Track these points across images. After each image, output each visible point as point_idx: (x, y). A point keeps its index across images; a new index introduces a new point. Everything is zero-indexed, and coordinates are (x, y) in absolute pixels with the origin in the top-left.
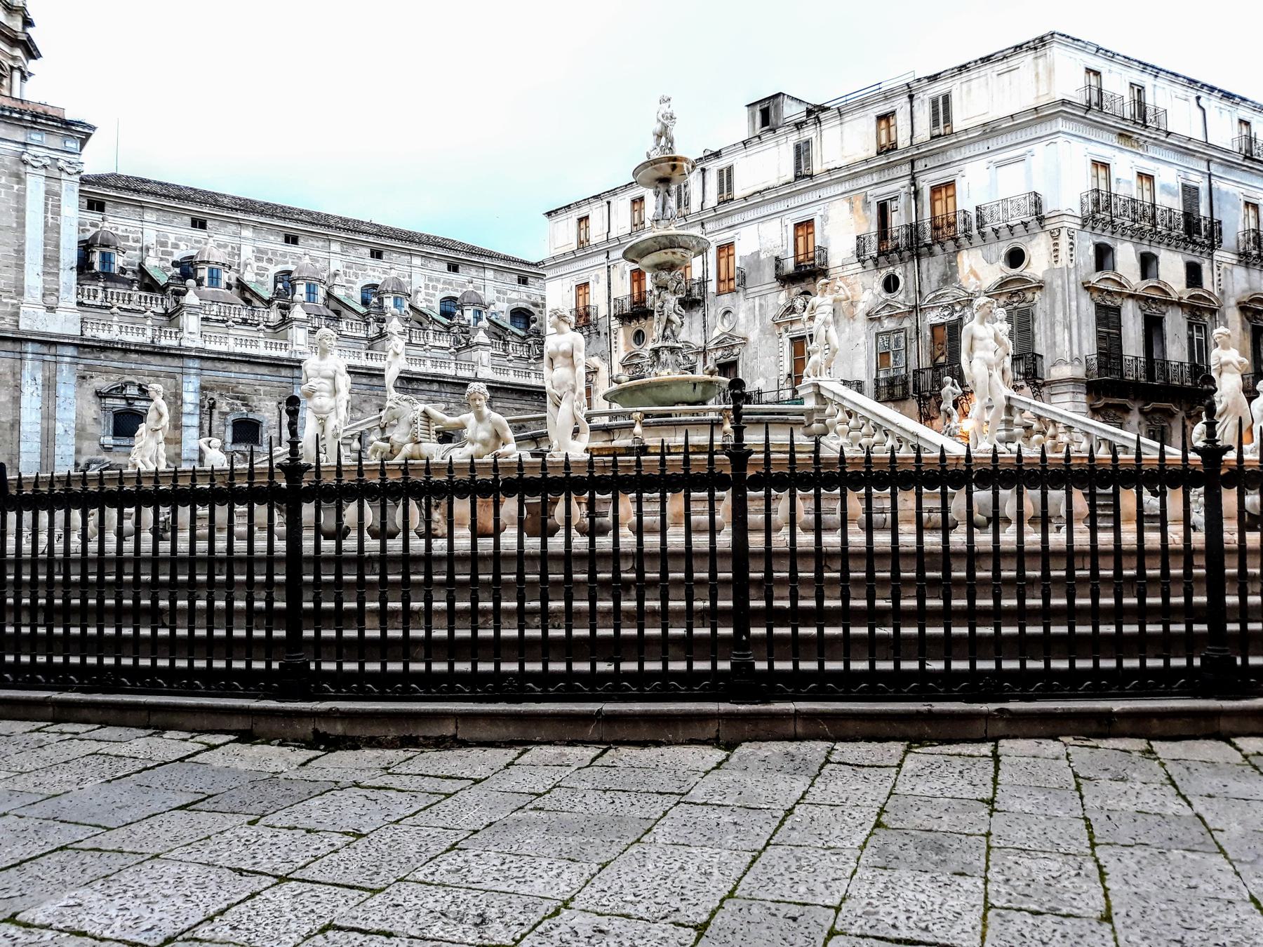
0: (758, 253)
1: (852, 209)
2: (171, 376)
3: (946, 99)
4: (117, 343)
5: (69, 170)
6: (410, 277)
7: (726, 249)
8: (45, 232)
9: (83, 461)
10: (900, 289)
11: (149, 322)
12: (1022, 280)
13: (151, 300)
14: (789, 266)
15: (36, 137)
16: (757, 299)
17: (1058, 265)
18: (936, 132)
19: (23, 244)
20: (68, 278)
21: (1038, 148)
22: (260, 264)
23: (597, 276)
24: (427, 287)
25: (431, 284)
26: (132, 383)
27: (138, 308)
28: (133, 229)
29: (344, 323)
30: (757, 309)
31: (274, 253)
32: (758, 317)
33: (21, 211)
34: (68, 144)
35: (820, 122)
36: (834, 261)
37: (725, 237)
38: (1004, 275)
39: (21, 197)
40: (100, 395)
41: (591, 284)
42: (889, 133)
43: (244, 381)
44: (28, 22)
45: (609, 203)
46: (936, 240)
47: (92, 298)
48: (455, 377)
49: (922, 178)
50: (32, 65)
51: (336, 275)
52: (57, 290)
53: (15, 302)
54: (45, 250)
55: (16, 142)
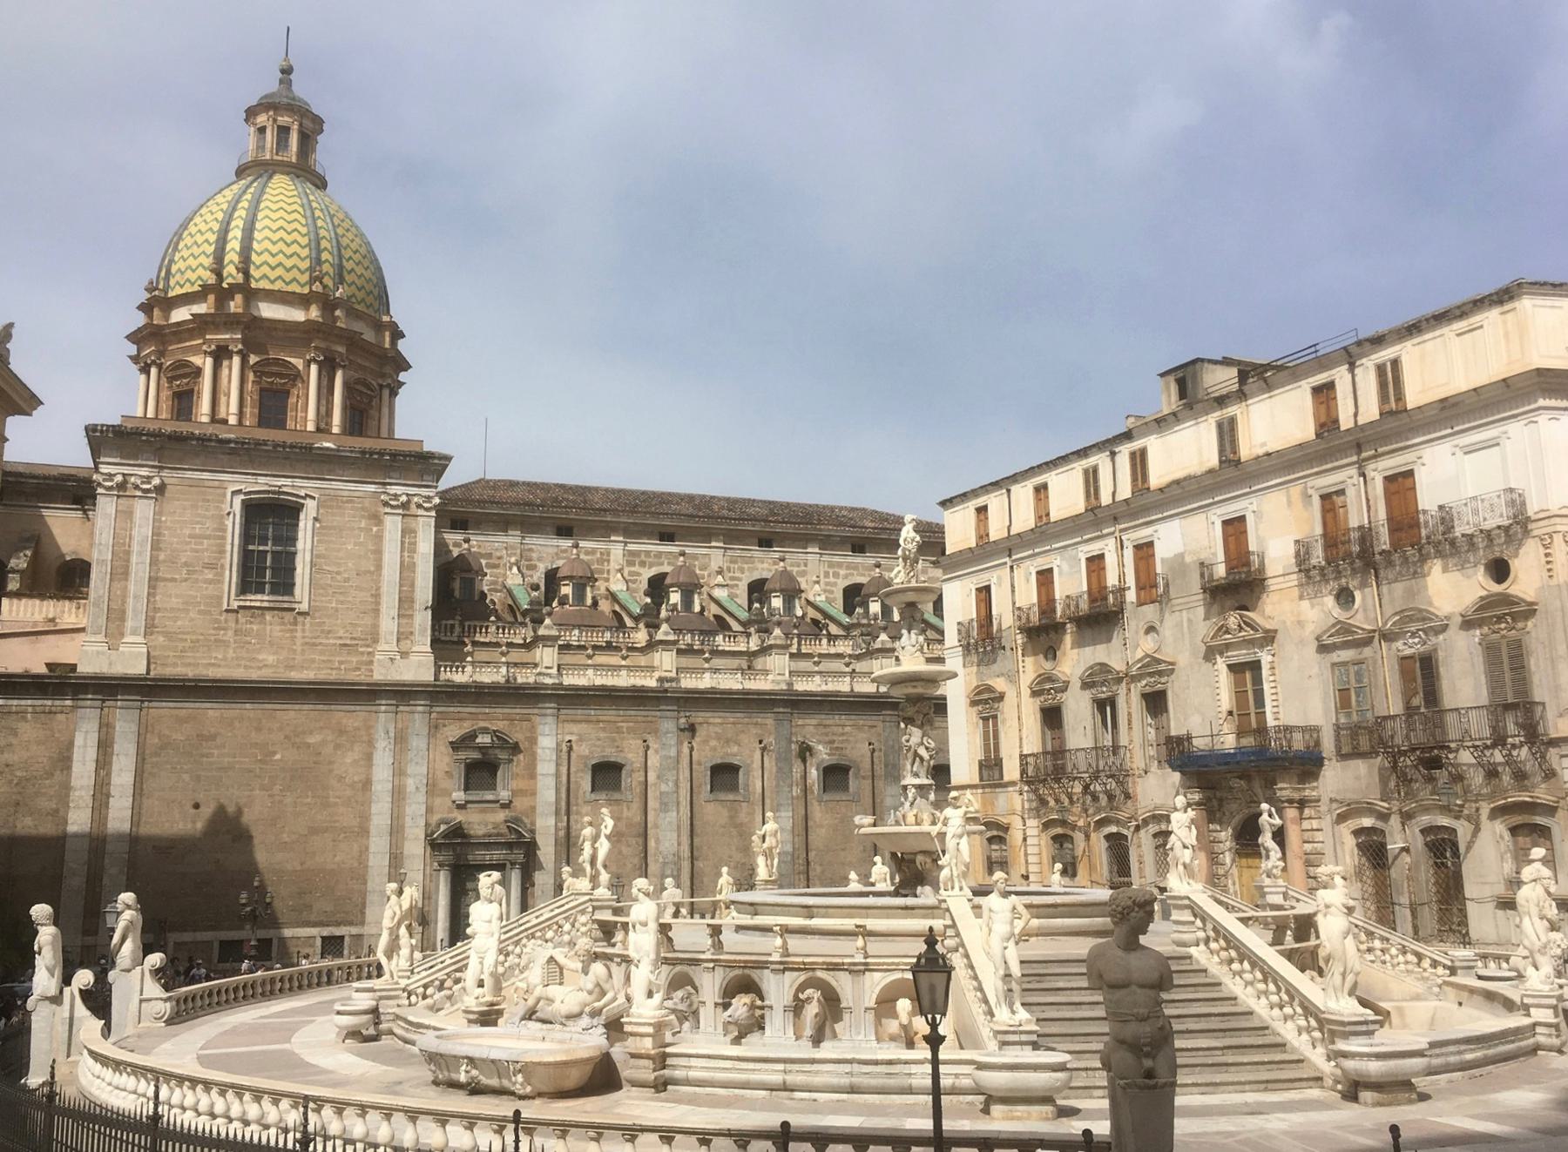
0: (1182, 555)
1: (1289, 503)
2: (526, 718)
3: (1395, 363)
4: (471, 687)
5: (426, 505)
6: (806, 565)
7: (1145, 551)
9: (435, 818)
10: (1356, 606)
12: (1506, 600)
14: (1221, 571)
16: (1184, 612)
17: (1554, 582)
18: (1387, 408)
19: (378, 589)
20: (423, 620)
21: (1515, 429)
22: (633, 569)
23: (999, 578)
24: (827, 575)
25: (831, 571)
26: (485, 731)
27: (494, 640)
30: (1185, 625)
31: (648, 553)
32: (1187, 636)
33: (378, 552)
36: (1272, 569)
37: (1143, 534)
38: (1484, 593)
39: (379, 538)
40: (456, 746)
42: (1328, 408)
43: (604, 718)
44: (398, 334)
46: (1396, 545)
48: (852, 694)
49: (1372, 466)
50: (402, 377)
52: (412, 633)
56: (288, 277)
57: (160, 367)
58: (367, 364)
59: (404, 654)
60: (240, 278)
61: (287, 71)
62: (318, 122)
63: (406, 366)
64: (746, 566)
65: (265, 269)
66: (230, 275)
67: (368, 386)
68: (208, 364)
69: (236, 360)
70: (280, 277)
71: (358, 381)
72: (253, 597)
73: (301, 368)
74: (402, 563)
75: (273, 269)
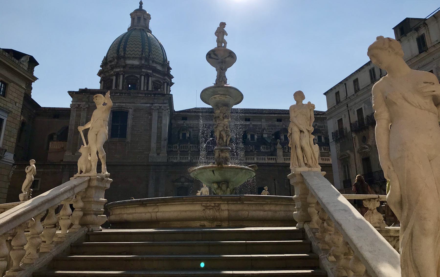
5: (165, 109)
11: (190, 155)
13: (194, 147)
15: (156, 101)
20: (164, 143)
28: (195, 124)
29: (262, 147)
33: (151, 124)
34: (165, 101)
35: (426, 25)
39: (151, 120)
41: (343, 119)
45: (345, 84)
47: (175, 149)
51: (263, 130)
52: (161, 148)
53: (148, 153)
54: (157, 135)
55: (150, 103)
57: (104, 81)
58: (159, 76)
59: (158, 154)
60: (122, 54)
63: (173, 77)
64: (273, 127)
65: (130, 52)
67: (160, 82)
68: (114, 78)
69: (121, 76)
71: (156, 81)
72: (114, 138)
73: (139, 77)
74: (158, 127)
75: (132, 51)
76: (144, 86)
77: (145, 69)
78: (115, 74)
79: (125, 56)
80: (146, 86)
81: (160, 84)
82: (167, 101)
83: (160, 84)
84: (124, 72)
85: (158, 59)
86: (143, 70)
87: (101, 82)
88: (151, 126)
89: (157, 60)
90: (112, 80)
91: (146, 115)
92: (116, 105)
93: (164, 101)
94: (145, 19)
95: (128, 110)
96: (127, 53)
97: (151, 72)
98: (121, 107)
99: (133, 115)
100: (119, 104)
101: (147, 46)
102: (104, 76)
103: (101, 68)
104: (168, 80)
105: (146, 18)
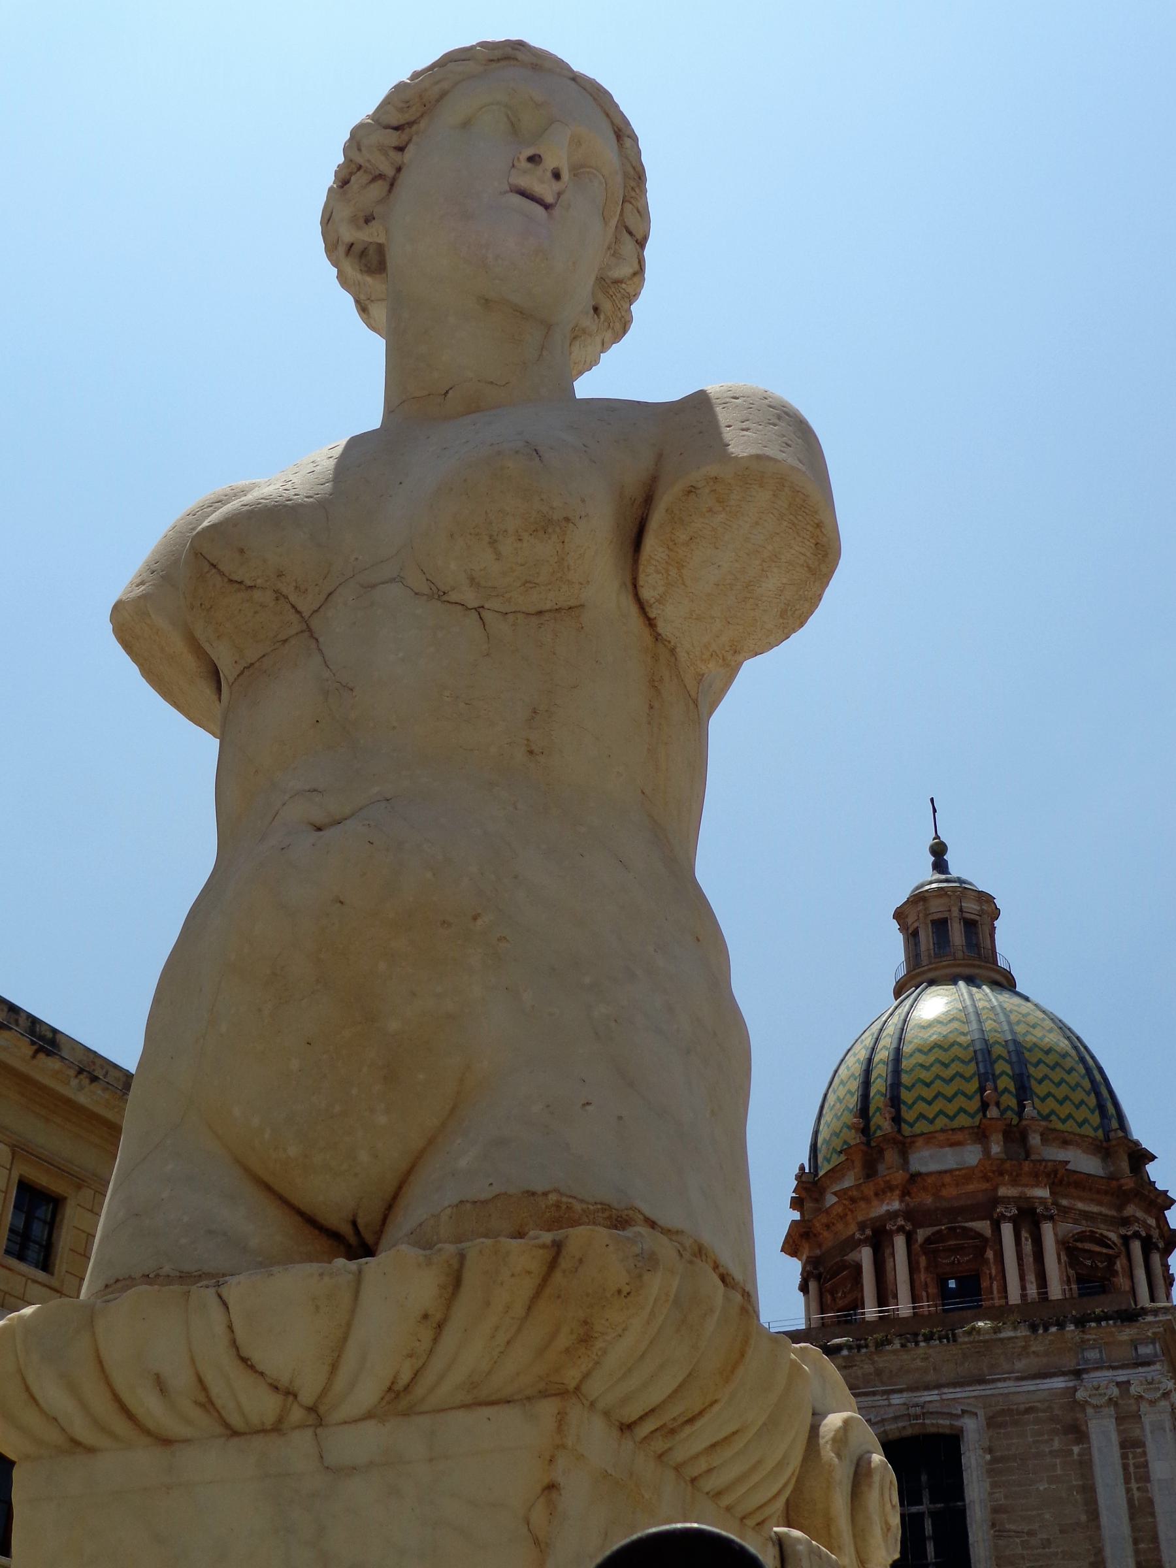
8: (1132, 1518)
15: (1092, 1355)
19: (1099, 1552)
33: (1089, 1491)
39: (1085, 1465)
44: (1141, 1157)
54: (1137, 1552)
55: (1063, 1374)
56: (951, 1109)
57: (818, 1278)
58: (1095, 1209)
61: (939, 851)
62: (985, 899)
65: (921, 1107)
66: (879, 1127)
67: (1102, 1241)
68: (865, 1256)
69: (900, 1242)
70: (941, 1112)
71: (1081, 1237)
73: (988, 1232)
74: (1130, 1501)
75: (930, 1103)
76: (1022, 1278)
77: (1015, 1182)
78: (868, 1232)
79: (899, 1131)
80: (1031, 1277)
81: (1105, 1250)
82: (1151, 1346)
83: (1105, 1250)
84: (908, 1214)
85: (1070, 1116)
86: (1003, 1191)
87: (804, 1288)
88: (1096, 1502)
89: (1064, 1121)
90: (858, 1268)
91: (1056, 1440)
92: (894, 1402)
93: (1139, 1351)
94: (970, 926)
95: (957, 1423)
96: (908, 1115)
97: (1043, 1193)
98: (918, 1410)
99: (990, 1450)
100: (905, 1395)
101: (1001, 1061)
102: (818, 1252)
103: (797, 1216)
104: (1148, 1227)
105: (977, 918)
